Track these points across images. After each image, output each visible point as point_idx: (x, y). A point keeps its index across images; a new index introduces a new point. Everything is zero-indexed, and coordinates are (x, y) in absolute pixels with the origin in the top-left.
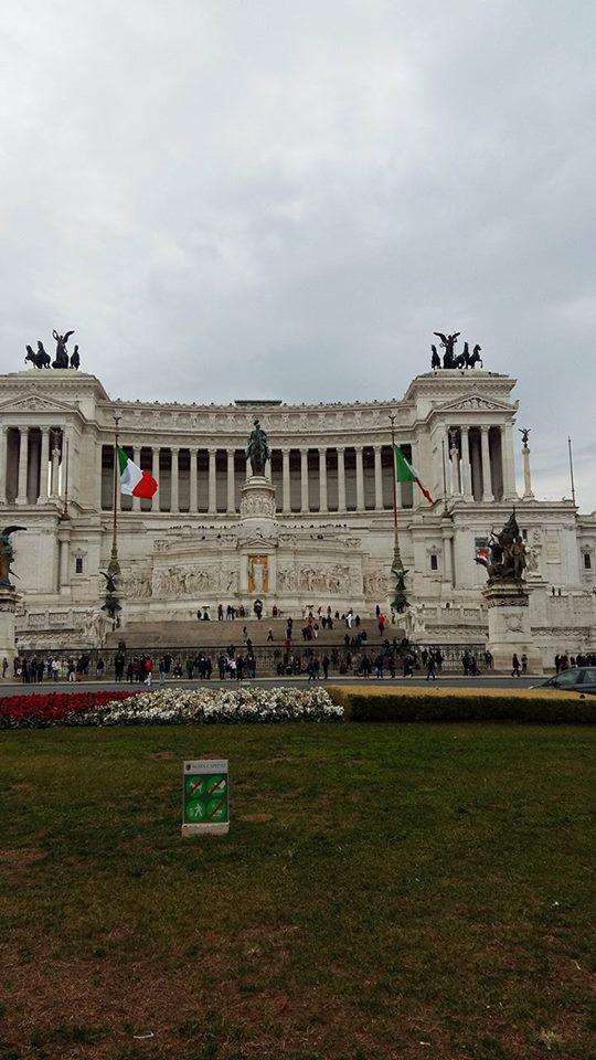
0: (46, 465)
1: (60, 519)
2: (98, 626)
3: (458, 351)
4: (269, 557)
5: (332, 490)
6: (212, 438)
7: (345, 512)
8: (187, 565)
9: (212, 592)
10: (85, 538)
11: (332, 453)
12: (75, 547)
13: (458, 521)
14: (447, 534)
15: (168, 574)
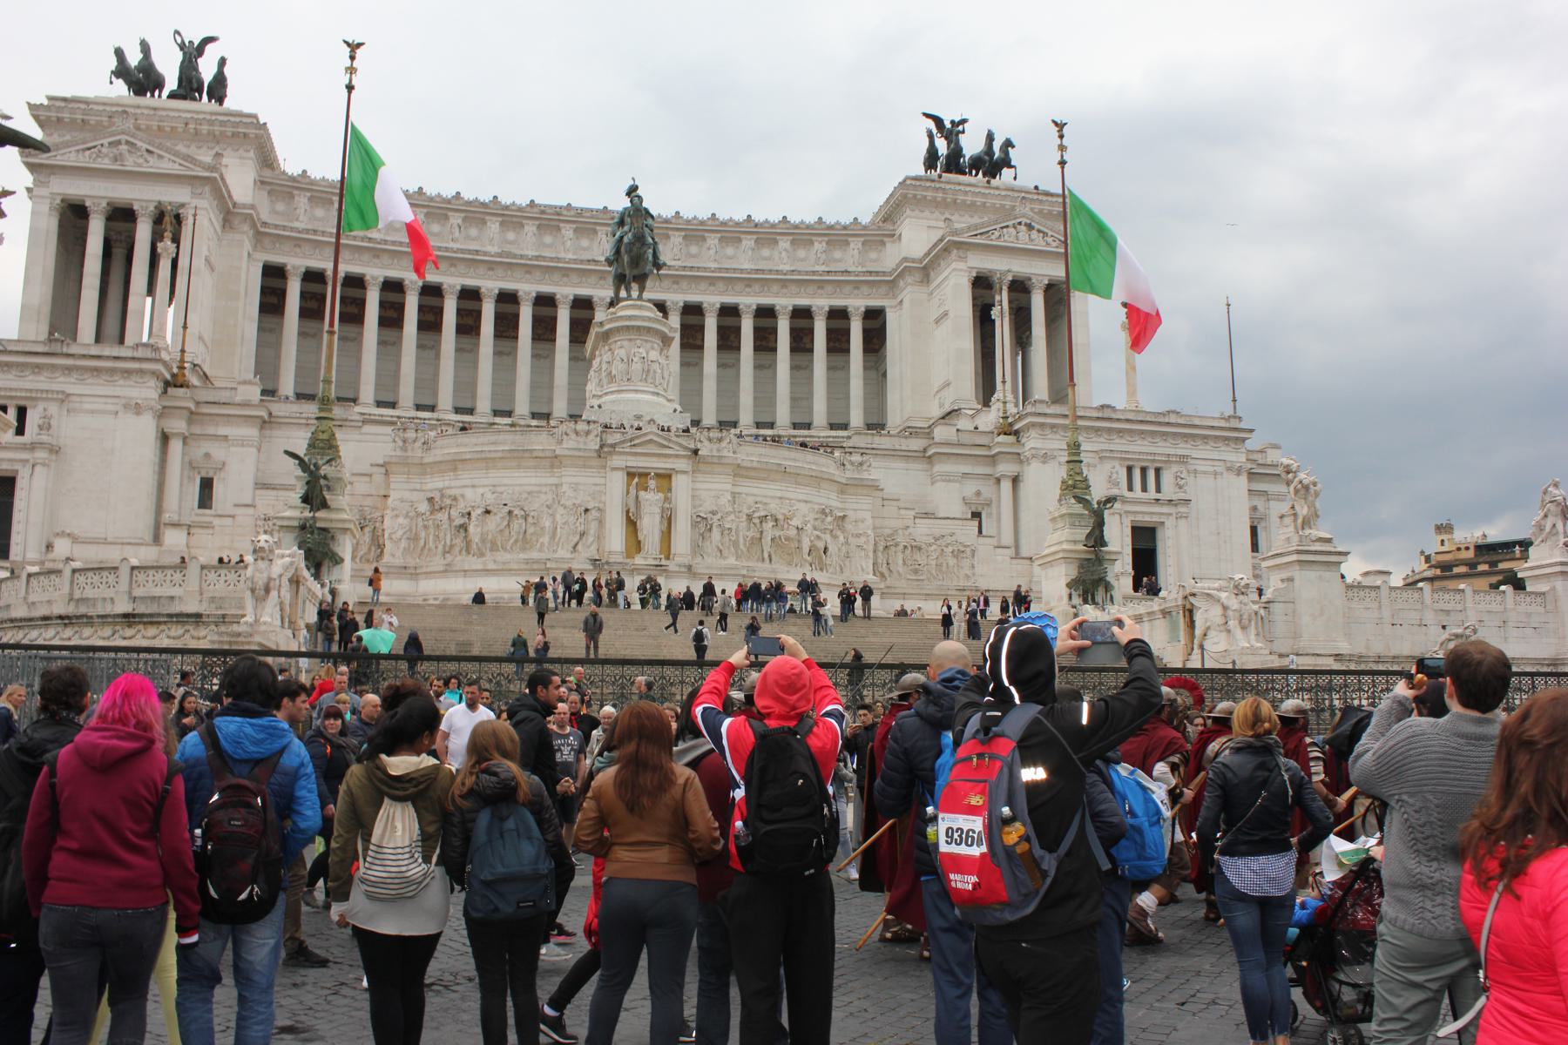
0: (141, 305)
1: (167, 384)
2: (286, 594)
3: (972, 145)
4: (680, 484)
5: (728, 391)
6: (491, 266)
7: (755, 431)
8: (473, 489)
9: (535, 555)
10: (222, 431)
11: (729, 312)
12: (199, 450)
13: (1032, 442)
14: (1006, 468)
15: (424, 507)
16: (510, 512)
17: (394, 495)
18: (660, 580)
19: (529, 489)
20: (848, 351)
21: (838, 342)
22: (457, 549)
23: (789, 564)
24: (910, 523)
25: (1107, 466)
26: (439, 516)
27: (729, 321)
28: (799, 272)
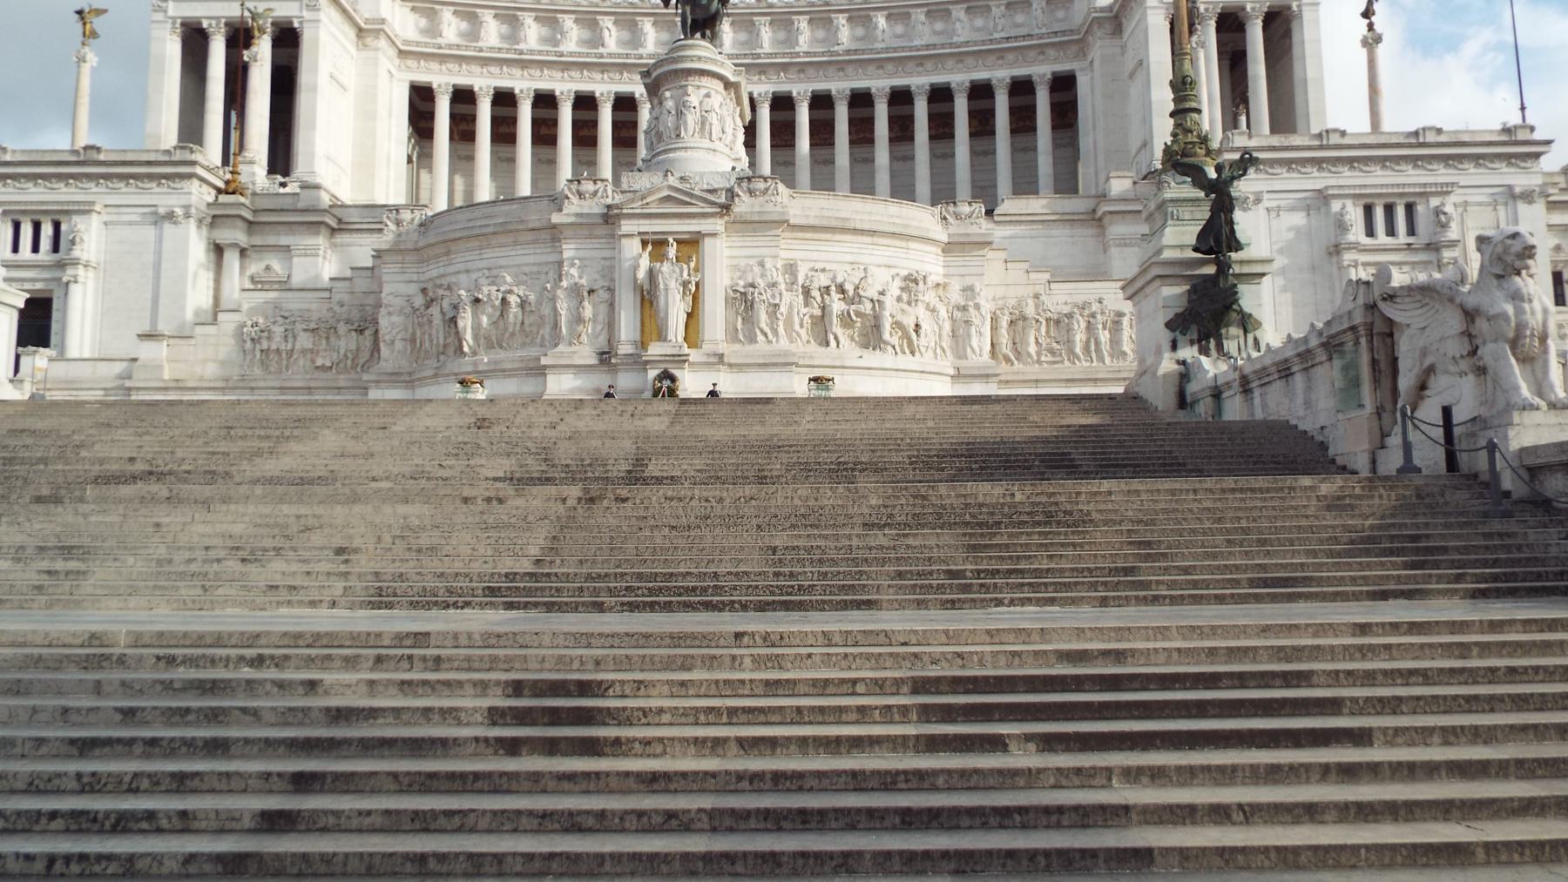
1: (219, 191)
9: (533, 352)
10: (284, 240)
15: (419, 301)
16: (504, 300)
17: (387, 289)
18: (676, 372)
19: (527, 269)
20: (1034, 129)
21: (1023, 121)
22: (451, 351)
23: (865, 346)
24: (1040, 289)
25: (1336, 206)
27: (903, 110)
28: (975, 43)
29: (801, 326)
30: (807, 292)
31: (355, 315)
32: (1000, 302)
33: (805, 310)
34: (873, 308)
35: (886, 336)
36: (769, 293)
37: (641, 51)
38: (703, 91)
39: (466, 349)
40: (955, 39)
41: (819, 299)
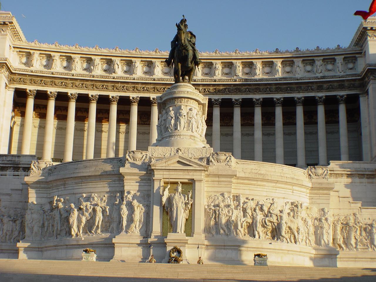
15: (47, 207)
18: (182, 249)
20: (338, 122)
26: (53, 213)
29: (242, 227)
30: (244, 211)
31: (12, 212)
32: (337, 218)
33: (243, 219)
34: (277, 219)
35: (283, 234)
36: (227, 210)
37: (134, 76)
38: (189, 108)
39: (73, 233)
40: (298, 76)
41: (250, 214)
